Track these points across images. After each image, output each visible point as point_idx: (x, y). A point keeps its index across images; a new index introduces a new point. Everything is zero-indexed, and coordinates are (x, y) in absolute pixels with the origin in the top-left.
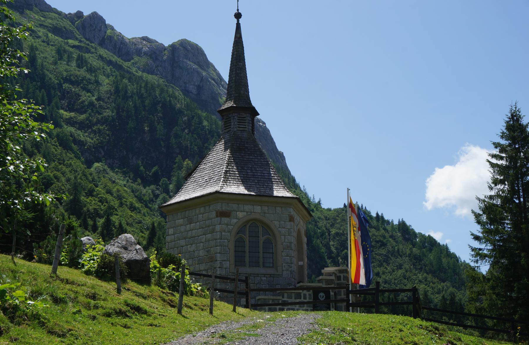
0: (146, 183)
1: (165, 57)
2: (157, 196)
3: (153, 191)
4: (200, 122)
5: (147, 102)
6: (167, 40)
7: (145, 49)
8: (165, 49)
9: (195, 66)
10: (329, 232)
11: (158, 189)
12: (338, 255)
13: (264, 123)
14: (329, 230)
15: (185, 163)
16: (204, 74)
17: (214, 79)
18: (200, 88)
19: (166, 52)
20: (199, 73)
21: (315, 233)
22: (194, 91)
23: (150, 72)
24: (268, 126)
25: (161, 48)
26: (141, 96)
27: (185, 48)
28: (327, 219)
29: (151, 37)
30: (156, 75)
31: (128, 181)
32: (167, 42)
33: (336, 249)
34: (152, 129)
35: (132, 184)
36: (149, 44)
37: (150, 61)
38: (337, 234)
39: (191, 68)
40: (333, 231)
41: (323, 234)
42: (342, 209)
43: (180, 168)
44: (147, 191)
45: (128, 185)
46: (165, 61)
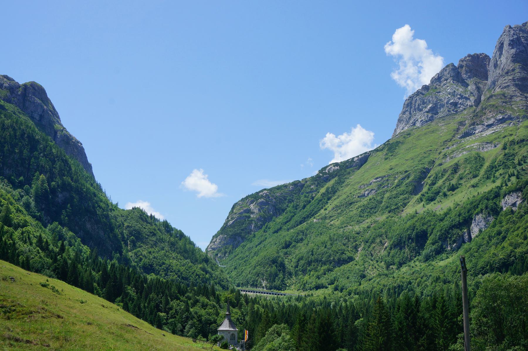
0: (15, 187)
1: (19, 93)
2: (22, 197)
3: (19, 193)
4: (51, 150)
5: (18, 134)
6: (21, 79)
7: (6, 85)
8: (19, 86)
9: (39, 101)
10: (123, 224)
11: (22, 192)
12: (128, 239)
13: (81, 144)
14: (123, 223)
15: (41, 176)
16: (45, 107)
17: (51, 111)
18: (41, 117)
19: (20, 89)
20: (42, 107)
21: (115, 225)
22: (37, 118)
23: (8, 101)
24: (84, 146)
25: (18, 86)
26: (14, 129)
27: (34, 88)
28: (122, 216)
29: (10, 76)
30: (13, 104)
31: (3, 185)
32: (21, 82)
33: (127, 235)
34: (21, 152)
35: (6, 188)
36: (8, 82)
37: (9, 94)
38: (128, 226)
39: (37, 103)
40: (126, 224)
41: (119, 226)
42: (131, 211)
43: (38, 179)
44: (16, 192)
45: (170, 315)
46: (19, 95)
